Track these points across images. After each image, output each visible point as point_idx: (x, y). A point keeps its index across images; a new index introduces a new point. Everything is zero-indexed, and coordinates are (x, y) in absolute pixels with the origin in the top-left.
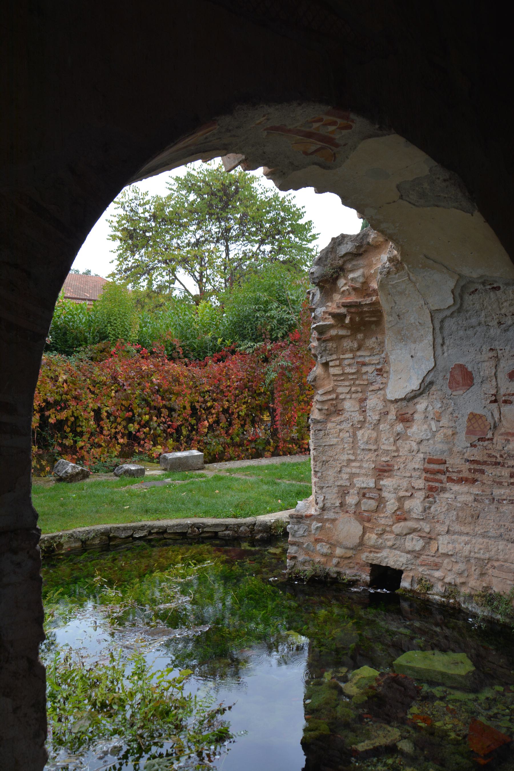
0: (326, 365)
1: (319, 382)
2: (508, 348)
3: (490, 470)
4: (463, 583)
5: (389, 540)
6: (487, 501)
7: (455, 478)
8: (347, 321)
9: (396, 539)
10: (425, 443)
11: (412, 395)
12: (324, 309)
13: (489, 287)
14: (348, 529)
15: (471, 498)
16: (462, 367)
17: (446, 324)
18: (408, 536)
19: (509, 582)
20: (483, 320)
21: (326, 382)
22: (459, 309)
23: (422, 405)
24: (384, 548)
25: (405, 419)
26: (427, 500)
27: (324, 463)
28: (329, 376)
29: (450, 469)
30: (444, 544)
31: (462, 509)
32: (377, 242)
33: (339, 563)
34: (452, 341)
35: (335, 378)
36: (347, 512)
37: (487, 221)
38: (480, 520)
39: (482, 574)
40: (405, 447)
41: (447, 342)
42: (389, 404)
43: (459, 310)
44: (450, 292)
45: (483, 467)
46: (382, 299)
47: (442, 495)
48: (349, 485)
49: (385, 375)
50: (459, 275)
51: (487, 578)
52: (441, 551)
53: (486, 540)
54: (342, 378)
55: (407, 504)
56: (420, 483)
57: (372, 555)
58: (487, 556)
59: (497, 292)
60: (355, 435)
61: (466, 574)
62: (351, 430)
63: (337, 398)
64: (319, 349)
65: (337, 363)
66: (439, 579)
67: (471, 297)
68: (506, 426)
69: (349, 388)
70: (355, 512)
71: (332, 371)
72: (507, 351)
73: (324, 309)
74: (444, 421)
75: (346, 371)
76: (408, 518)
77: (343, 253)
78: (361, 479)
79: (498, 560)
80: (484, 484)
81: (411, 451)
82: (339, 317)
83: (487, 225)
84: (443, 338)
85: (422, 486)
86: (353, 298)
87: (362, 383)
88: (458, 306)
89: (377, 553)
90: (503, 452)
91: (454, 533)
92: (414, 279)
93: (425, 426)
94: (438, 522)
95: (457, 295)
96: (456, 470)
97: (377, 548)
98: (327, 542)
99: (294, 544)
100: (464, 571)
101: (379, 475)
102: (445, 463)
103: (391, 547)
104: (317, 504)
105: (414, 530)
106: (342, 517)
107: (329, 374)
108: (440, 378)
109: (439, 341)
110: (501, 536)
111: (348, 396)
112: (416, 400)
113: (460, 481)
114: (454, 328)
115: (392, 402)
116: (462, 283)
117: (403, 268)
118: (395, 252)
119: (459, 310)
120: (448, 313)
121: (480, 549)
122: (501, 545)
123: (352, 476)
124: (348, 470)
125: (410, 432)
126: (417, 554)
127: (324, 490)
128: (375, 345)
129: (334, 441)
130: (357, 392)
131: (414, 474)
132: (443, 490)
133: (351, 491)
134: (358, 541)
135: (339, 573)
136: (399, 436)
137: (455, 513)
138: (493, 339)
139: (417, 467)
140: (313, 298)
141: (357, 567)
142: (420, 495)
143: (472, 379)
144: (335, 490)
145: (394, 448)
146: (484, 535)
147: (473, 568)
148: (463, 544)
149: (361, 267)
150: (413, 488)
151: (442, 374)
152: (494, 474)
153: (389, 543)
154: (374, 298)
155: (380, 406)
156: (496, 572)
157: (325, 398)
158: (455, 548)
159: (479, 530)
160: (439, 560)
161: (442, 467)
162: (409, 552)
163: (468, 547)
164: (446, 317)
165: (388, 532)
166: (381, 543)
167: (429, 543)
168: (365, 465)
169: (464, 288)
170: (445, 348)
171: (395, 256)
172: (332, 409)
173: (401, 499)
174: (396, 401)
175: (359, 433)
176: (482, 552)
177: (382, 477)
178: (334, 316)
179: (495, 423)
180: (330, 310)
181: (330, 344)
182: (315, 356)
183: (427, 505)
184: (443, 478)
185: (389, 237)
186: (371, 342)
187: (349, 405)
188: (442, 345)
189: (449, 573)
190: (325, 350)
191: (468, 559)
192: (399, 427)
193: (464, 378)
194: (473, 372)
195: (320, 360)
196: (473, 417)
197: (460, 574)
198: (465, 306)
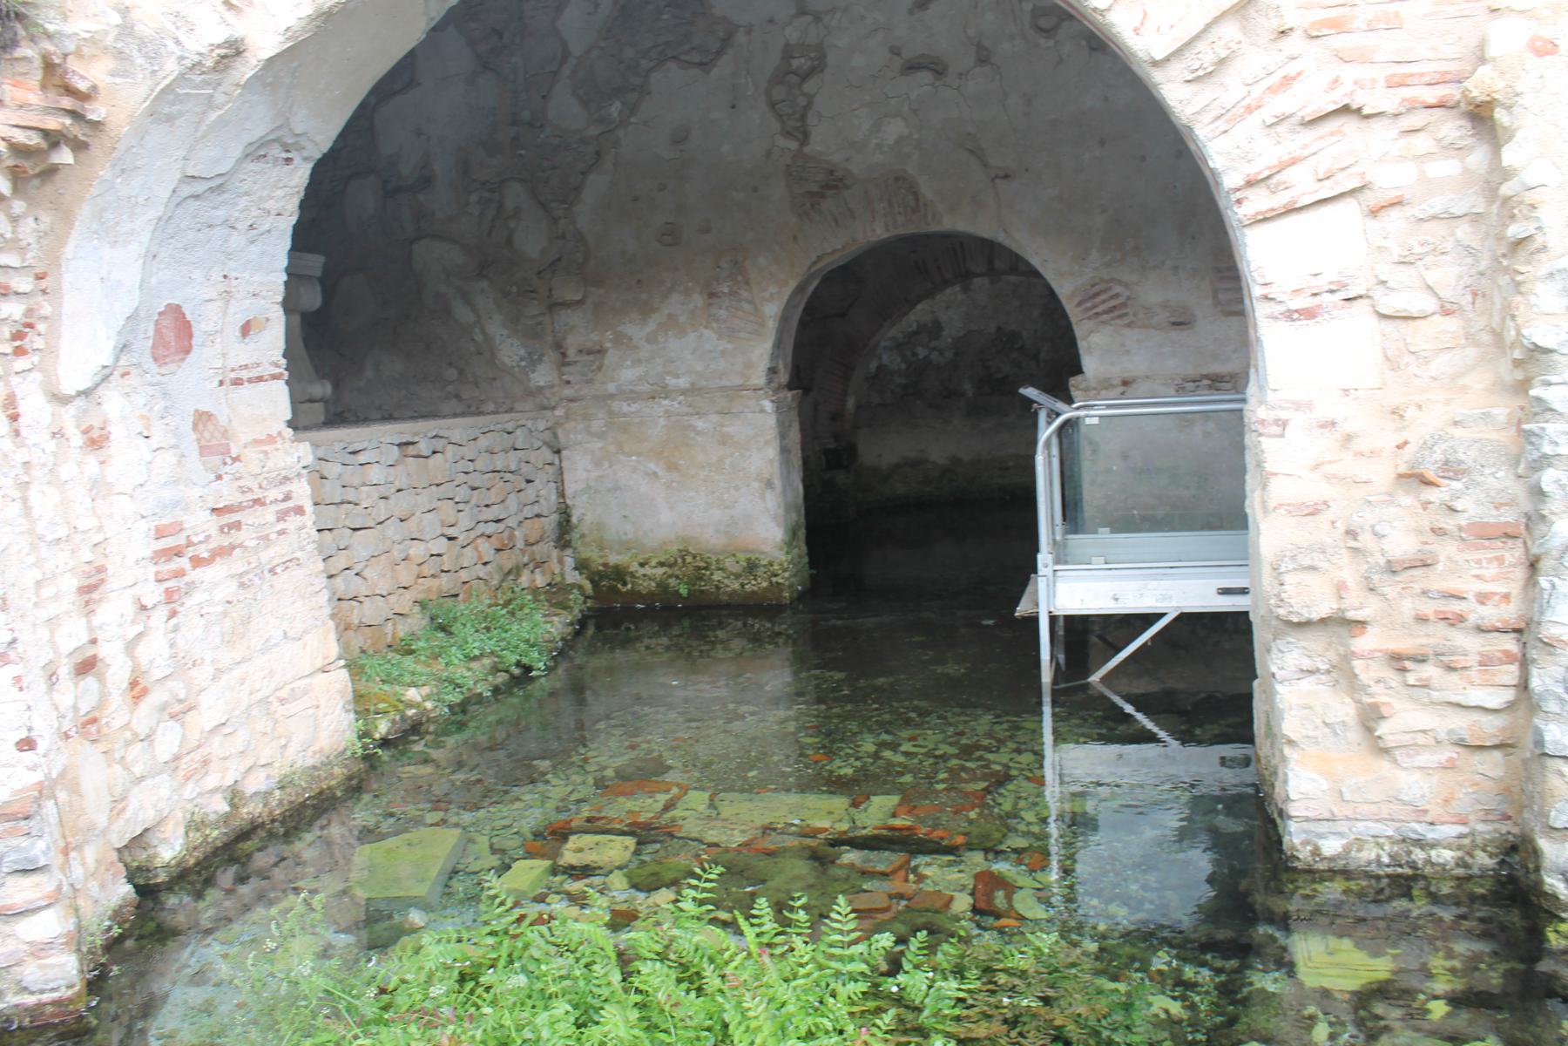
3: (248, 518)
6: (257, 581)
7: (206, 555)
15: (234, 584)
16: (175, 312)
25: (96, 442)
29: (195, 540)
31: (225, 614)
45: (235, 517)
49: (41, 327)
96: (201, 538)
101: (87, 603)
136: (99, 488)
146: (265, 650)
156: (292, 708)
161: (179, 540)
173: (130, 647)
177: (92, 606)
184: (184, 562)
196: (202, 419)
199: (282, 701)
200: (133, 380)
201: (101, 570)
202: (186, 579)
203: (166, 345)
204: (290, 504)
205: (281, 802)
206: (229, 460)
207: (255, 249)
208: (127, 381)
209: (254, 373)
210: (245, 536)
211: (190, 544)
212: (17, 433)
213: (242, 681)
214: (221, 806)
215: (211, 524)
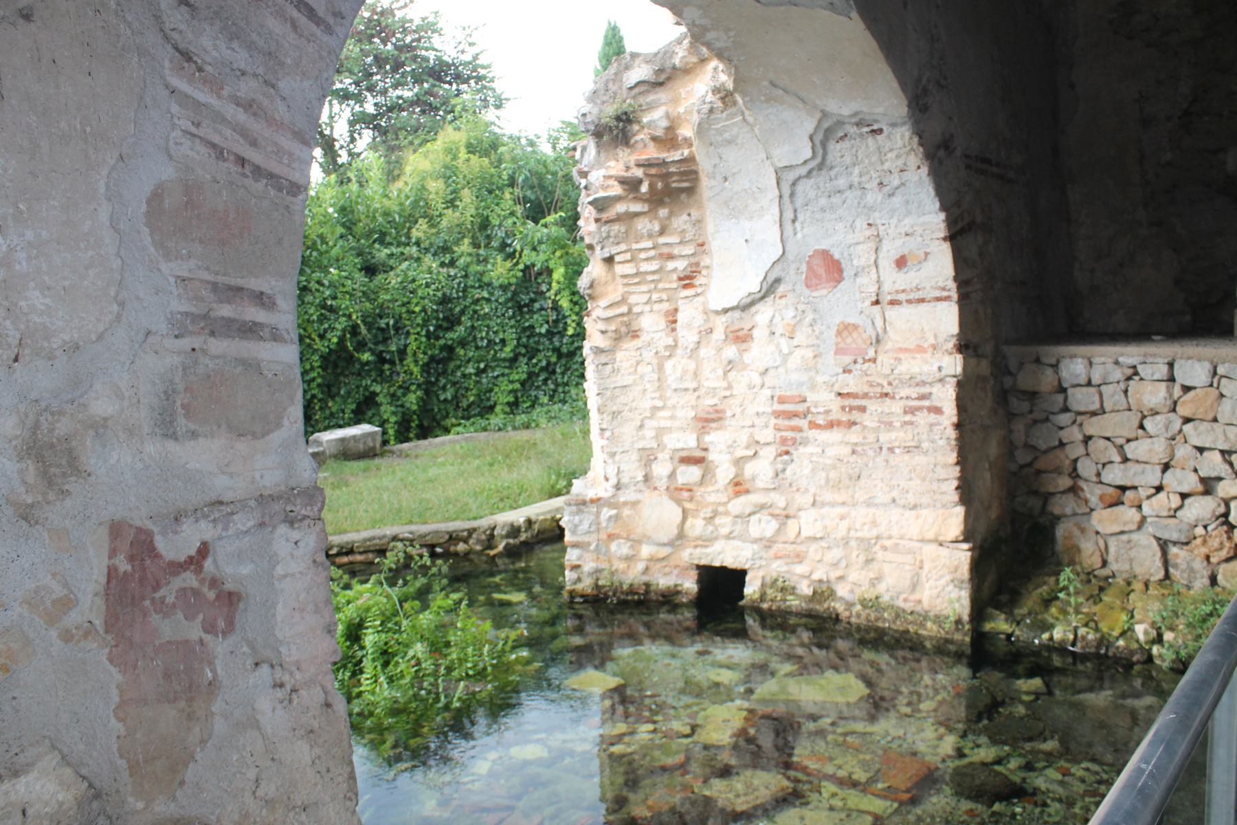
0: (609, 260)
1: (599, 290)
2: (894, 221)
3: (873, 406)
4: (841, 578)
5: (723, 526)
6: (871, 453)
7: (821, 422)
8: (644, 188)
9: (734, 523)
10: (771, 372)
11: (749, 300)
12: (603, 172)
13: (866, 129)
14: (659, 515)
15: (848, 450)
16: (825, 255)
17: (799, 188)
18: (753, 518)
19: (907, 567)
20: (856, 180)
21: (610, 288)
22: (820, 164)
23: (763, 314)
24: (716, 538)
25: (741, 338)
26: (779, 459)
27: (615, 415)
28: (614, 279)
29: (813, 410)
30: (808, 523)
31: (834, 467)
32: (687, 63)
33: (647, 568)
34: (808, 214)
35: (625, 281)
36: (655, 488)
37: (869, 28)
38: (862, 481)
39: (868, 561)
40: (741, 381)
41: (801, 217)
42: (712, 317)
43: (821, 166)
44: (807, 139)
46: (698, 150)
47: (802, 449)
48: (655, 446)
49: (704, 272)
50: (822, 111)
51: (875, 566)
52: (804, 534)
53: (872, 510)
54: (636, 280)
55: (749, 469)
56: (767, 435)
57: (698, 550)
58: (874, 533)
59: (878, 137)
60: (661, 368)
61: (843, 564)
62: (655, 361)
63: (630, 312)
64: (597, 236)
65: (628, 256)
66: (803, 577)
67: (838, 146)
68: (894, 339)
69: (647, 296)
71: (619, 269)
72: (892, 226)
73: (603, 172)
74: (800, 338)
75: (642, 270)
77: (633, 82)
78: (674, 435)
79: (890, 538)
80: (865, 427)
81: (751, 387)
82: (631, 185)
83: (867, 34)
84: (795, 211)
85: (770, 439)
86: (652, 152)
87: (668, 286)
88: (819, 160)
89: (706, 547)
90: (892, 377)
91: (823, 504)
92: (750, 119)
93: (772, 348)
94: (798, 490)
95: (817, 142)
96: (821, 410)
97: (707, 541)
98: (628, 539)
99: (575, 545)
102: (805, 401)
103: (728, 537)
104: (607, 479)
105: (762, 507)
106: (648, 497)
107: (614, 274)
108: (792, 272)
109: (789, 215)
110: (894, 501)
111: (647, 308)
112: (753, 309)
113: (831, 425)
114: (812, 194)
115: (717, 313)
116: (826, 125)
117: (735, 103)
118: (723, 78)
119: (821, 166)
120: (803, 171)
121: (864, 524)
122: (895, 513)
123: (660, 432)
124: (654, 423)
125: (747, 357)
126: (769, 543)
127: (617, 457)
128: (688, 227)
129: (628, 380)
130: (661, 301)
131: (757, 421)
132: (805, 442)
133: (660, 456)
134: (675, 532)
135: (647, 585)
137: (824, 475)
138: (871, 209)
139: (761, 410)
140: (582, 156)
141: (676, 572)
142: (768, 453)
143: (840, 270)
144: (635, 456)
145: (725, 384)
146: (869, 503)
147: (854, 554)
148: (837, 520)
149: (662, 104)
150: (758, 442)
151: (793, 266)
152: (880, 410)
153: (724, 531)
154: (686, 152)
155: (699, 320)
156: (889, 556)
157: (610, 313)
158: (825, 527)
159: (861, 496)
160: (802, 548)
161: (801, 408)
162: (756, 541)
163: (845, 523)
164: (800, 178)
165: (721, 514)
167: (785, 524)
168: (680, 413)
169: (828, 133)
170: (797, 224)
171: (723, 84)
172: (623, 329)
173: (739, 462)
174: (726, 311)
175: (668, 365)
176: (866, 527)
178: (623, 181)
179: (877, 336)
180: (613, 172)
181: (616, 227)
182: (591, 247)
183: (780, 467)
184: (803, 423)
185: (720, 55)
186: (681, 221)
187: (652, 323)
188: (794, 221)
189: (819, 565)
190: (608, 237)
191: (846, 542)
192: (731, 351)
193: (830, 269)
194: (842, 261)
195: (599, 254)
196: (846, 329)
197: (835, 565)
198: (830, 158)
199: (885, 548)
200: (791, 298)
201: (723, 411)
202: (804, 435)
203: (818, 277)
204: (926, 403)
205: (858, 616)
206: (860, 361)
207: (897, 200)
208: (783, 301)
209: (919, 295)
210: (868, 420)
211: (808, 411)
212: (674, 330)
213: (842, 518)
214: (805, 589)
215: (835, 404)
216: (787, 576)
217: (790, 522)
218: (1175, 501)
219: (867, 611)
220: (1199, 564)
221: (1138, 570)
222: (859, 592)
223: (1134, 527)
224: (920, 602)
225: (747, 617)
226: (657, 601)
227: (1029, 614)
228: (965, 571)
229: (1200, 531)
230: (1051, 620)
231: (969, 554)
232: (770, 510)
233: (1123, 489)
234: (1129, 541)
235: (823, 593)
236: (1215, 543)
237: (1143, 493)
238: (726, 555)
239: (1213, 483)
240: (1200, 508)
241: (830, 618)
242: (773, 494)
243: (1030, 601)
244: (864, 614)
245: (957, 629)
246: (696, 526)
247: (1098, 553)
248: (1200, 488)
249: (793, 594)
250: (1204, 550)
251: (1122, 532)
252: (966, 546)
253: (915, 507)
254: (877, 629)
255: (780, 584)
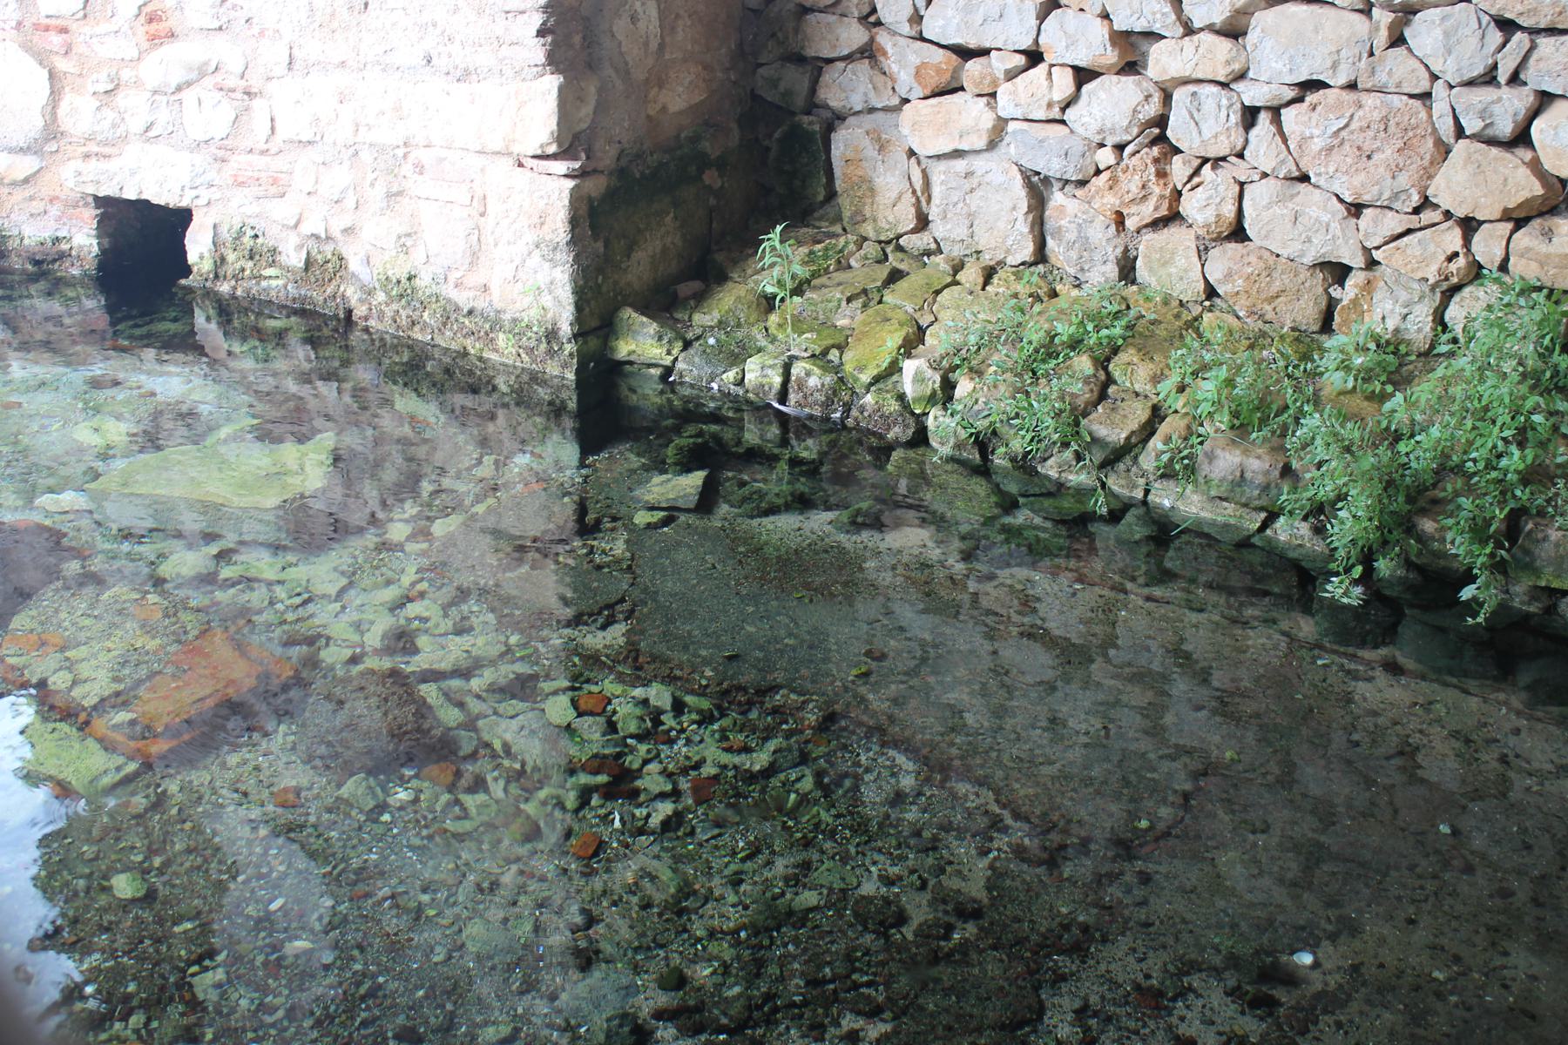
4: (348, 231)
18: (189, 96)
24: (125, 138)
39: (393, 196)
52: (282, 133)
70: (19, 24)
76: (177, 31)
100: (347, 188)
126: (222, 152)
141: (54, 211)
153: (136, 125)
160: (279, 163)
166: (114, 126)
216: (261, 225)
217: (257, 103)
218: (1064, 83)
219: (395, 306)
220: (1100, 233)
221: (984, 240)
222: (378, 267)
223: (981, 143)
224: (485, 288)
225: (197, 312)
226: (24, 271)
227: (721, 324)
228: (558, 226)
229: (1106, 157)
230: (762, 342)
231: (571, 183)
232: (218, 78)
233: (965, 53)
234: (969, 175)
235: (322, 266)
236: (1132, 185)
237: (1000, 63)
238: (152, 180)
239: (1143, 44)
240: (1113, 105)
241: (336, 316)
242: (220, 40)
243: (729, 300)
244: (389, 313)
245: (551, 353)
246: (79, 113)
247: (909, 199)
248: (1111, 57)
249: (273, 264)
250: (1111, 201)
251: (957, 154)
252: (561, 167)
253: (465, 75)
254: (411, 345)
255: (247, 241)
